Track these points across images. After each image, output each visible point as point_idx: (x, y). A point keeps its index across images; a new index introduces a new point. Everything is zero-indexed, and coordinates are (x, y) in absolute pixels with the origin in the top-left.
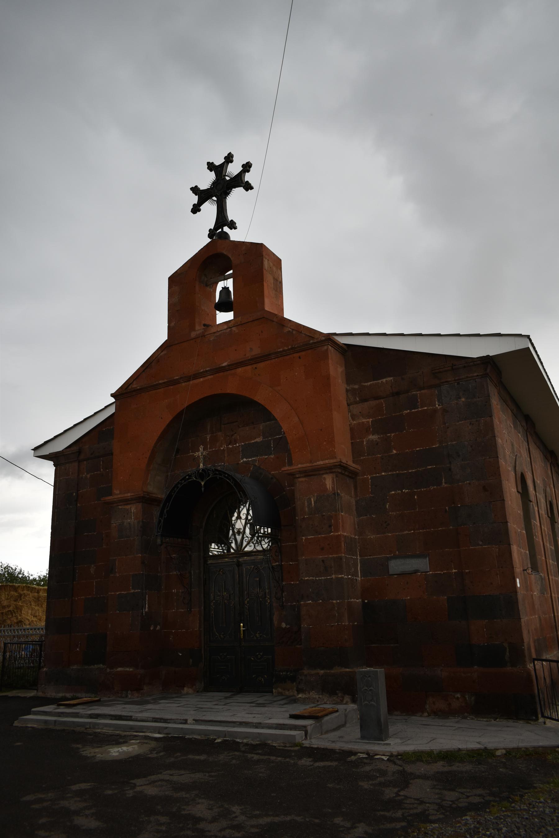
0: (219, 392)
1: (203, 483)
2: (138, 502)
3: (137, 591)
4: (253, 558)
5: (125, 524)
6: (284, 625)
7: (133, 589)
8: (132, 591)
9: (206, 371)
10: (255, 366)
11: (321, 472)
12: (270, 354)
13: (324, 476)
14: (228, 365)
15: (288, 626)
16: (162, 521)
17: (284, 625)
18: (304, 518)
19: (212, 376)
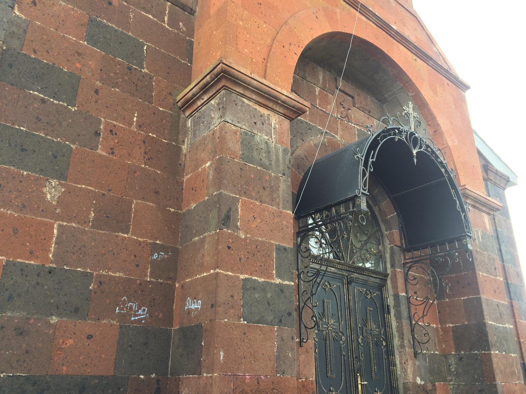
0: (386, 51)
1: (415, 152)
2: (285, 116)
3: (286, 282)
4: (364, 277)
5: (257, 138)
6: (419, 381)
7: (279, 276)
8: (278, 281)
9: (374, 15)
10: (415, 57)
11: (484, 209)
12: (431, 59)
13: (483, 214)
14: (397, 32)
15: (423, 383)
16: (368, 174)
17: (419, 381)
18: (476, 250)
19: (375, 26)
